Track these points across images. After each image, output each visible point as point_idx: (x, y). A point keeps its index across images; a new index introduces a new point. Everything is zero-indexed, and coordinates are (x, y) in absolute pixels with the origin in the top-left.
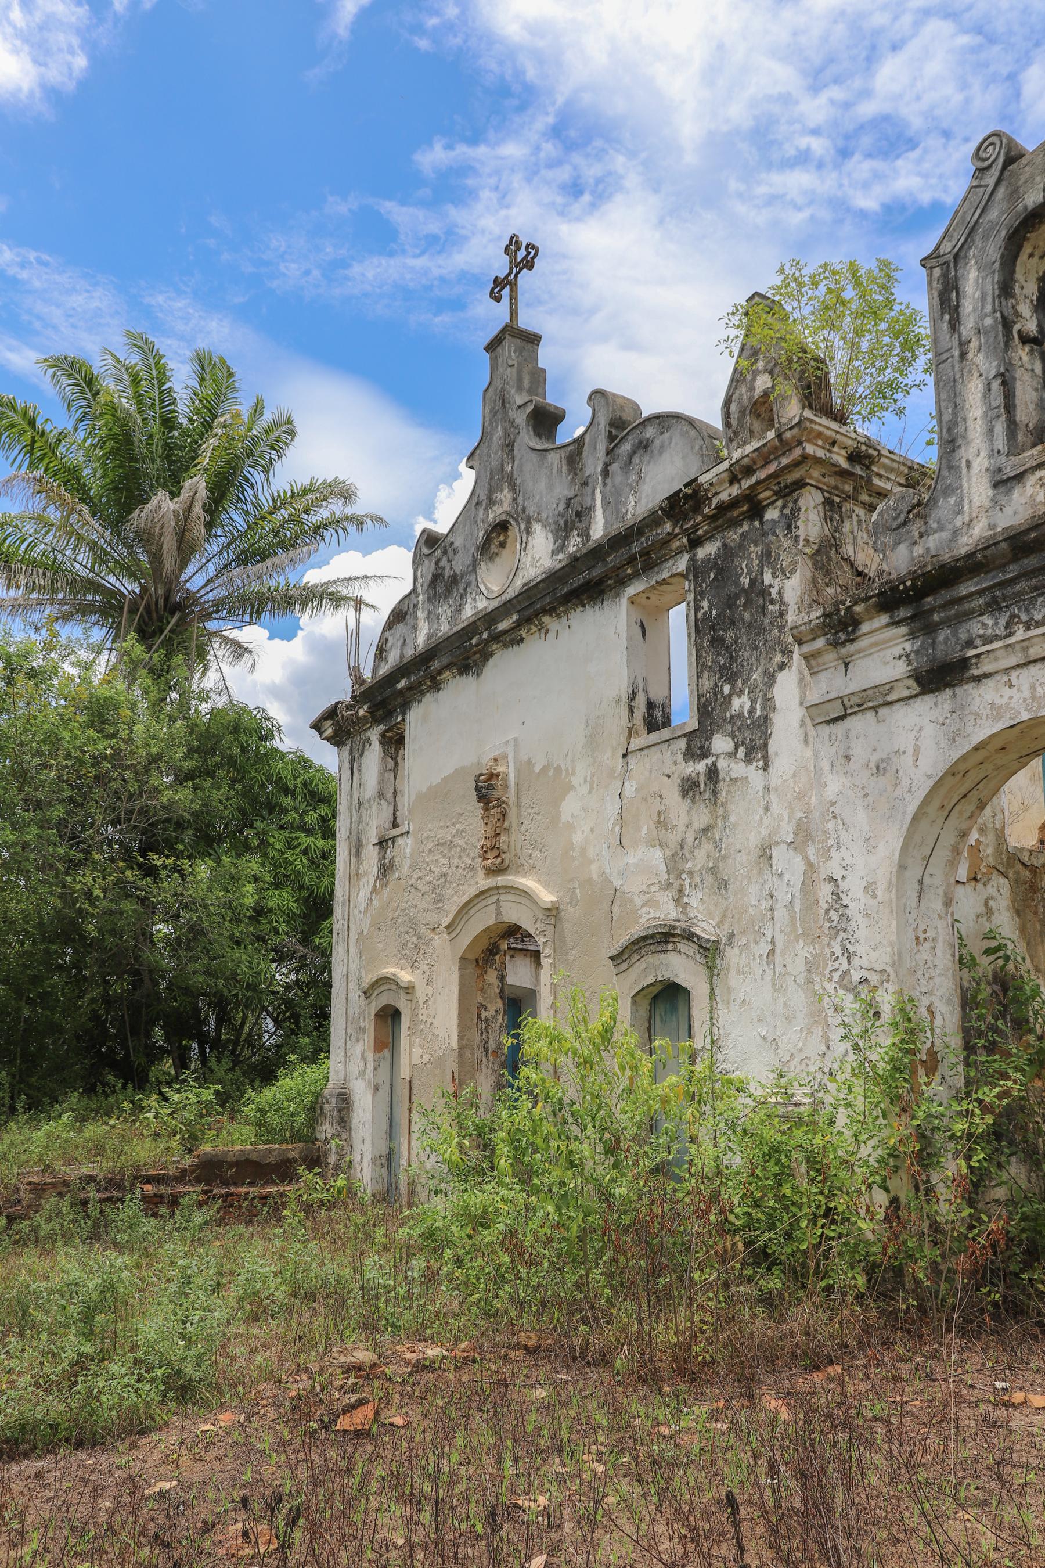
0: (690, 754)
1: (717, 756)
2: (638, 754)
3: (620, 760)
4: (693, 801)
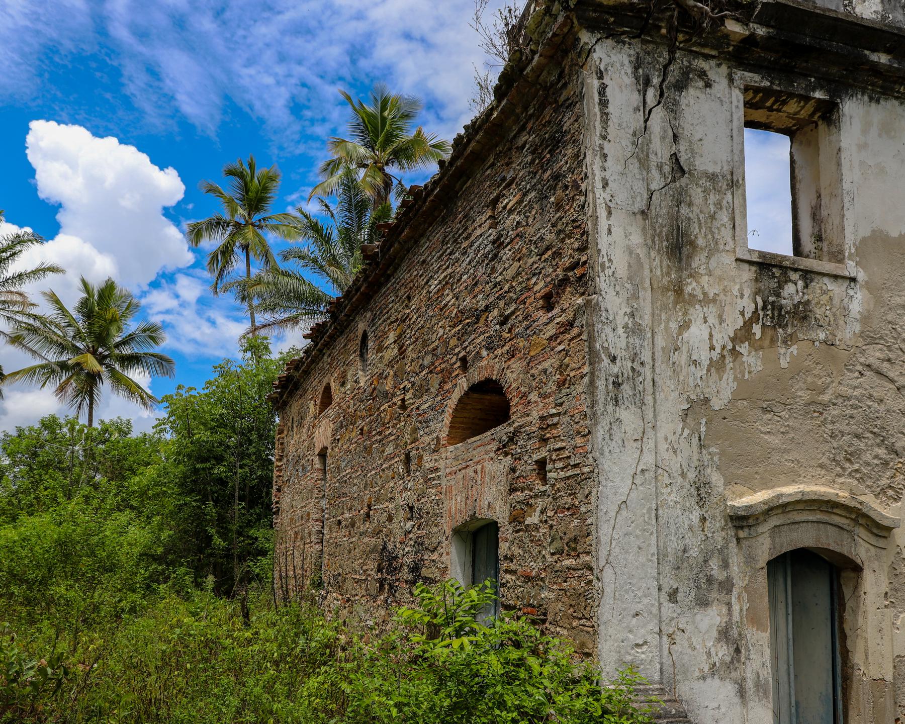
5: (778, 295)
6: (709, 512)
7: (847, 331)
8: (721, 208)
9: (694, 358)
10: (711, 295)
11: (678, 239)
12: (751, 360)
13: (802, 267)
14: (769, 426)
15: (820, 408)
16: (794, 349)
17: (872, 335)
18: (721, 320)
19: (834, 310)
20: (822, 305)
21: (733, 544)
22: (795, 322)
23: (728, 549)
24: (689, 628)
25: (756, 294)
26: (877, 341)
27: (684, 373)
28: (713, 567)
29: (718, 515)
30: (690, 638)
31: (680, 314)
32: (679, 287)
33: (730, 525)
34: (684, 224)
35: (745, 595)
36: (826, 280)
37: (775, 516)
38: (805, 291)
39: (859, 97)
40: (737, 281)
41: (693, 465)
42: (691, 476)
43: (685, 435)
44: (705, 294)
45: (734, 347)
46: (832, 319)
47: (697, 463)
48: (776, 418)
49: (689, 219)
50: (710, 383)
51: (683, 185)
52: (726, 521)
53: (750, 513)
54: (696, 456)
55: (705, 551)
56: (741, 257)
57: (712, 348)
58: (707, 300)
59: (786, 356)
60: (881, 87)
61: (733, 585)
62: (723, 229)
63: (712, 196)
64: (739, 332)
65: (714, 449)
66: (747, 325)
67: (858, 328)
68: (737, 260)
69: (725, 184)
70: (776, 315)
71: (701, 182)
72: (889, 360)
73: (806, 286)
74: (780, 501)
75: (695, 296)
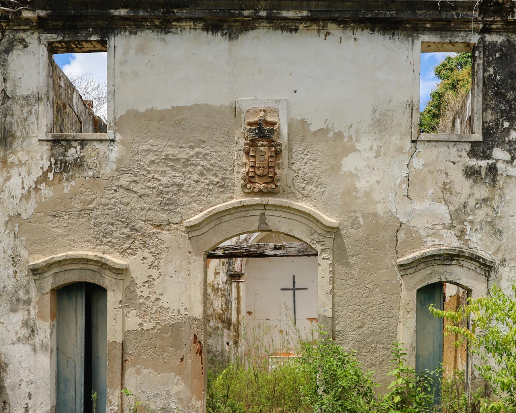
0: (472, 154)
1: (497, 160)
2: (427, 144)
3: (409, 144)
4: (475, 181)
5: (65, 155)
6: (19, 269)
7: (107, 169)
8: (31, 114)
9: (12, 194)
10: (23, 161)
11: (4, 135)
12: (46, 191)
13: (79, 139)
14: (57, 224)
15: (88, 212)
16: (73, 183)
17: (124, 169)
18: (29, 173)
19: (99, 159)
20: (92, 157)
21: (32, 283)
22: (75, 169)
23: (29, 285)
24: (6, 322)
25: (51, 156)
26: (128, 172)
27: (6, 203)
28: (20, 293)
29: (24, 269)
30: (7, 326)
31: (5, 173)
32: (5, 160)
33: (31, 273)
34: (8, 126)
35: (37, 306)
36: (95, 143)
37: (55, 268)
38: (81, 151)
39: (122, 33)
40: (40, 151)
41: (10, 247)
42: (9, 252)
43: (6, 233)
44: (20, 161)
45: (36, 186)
46: (98, 164)
47: (13, 246)
48: (61, 219)
49: (11, 123)
50: (22, 206)
51: (8, 105)
52: (29, 272)
53: (36, 267)
54: (12, 242)
55: (16, 287)
56: (41, 139)
57: (23, 188)
58: (21, 164)
59: (67, 187)
60: (135, 25)
61: (31, 302)
62: (31, 125)
63: (26, 108)
64: (39, 178)
65: (23, 238)
66: (45, 174)
67: (114, 167)
68: (39, 140)
69: (34, 100)
70: (63, 166)
71: (19, 102)
72: (135, 181)
73: (82, 148)
74: (53, 260)
75: (14, 163)
